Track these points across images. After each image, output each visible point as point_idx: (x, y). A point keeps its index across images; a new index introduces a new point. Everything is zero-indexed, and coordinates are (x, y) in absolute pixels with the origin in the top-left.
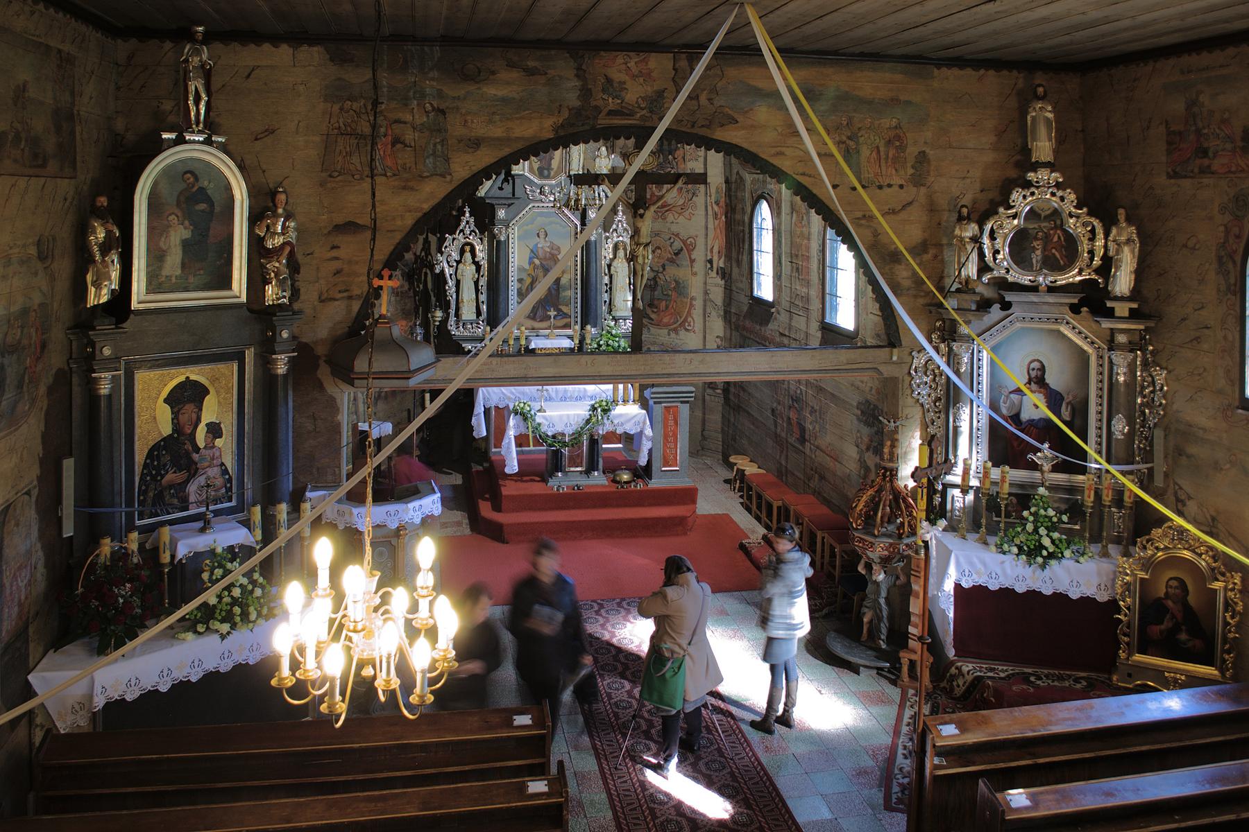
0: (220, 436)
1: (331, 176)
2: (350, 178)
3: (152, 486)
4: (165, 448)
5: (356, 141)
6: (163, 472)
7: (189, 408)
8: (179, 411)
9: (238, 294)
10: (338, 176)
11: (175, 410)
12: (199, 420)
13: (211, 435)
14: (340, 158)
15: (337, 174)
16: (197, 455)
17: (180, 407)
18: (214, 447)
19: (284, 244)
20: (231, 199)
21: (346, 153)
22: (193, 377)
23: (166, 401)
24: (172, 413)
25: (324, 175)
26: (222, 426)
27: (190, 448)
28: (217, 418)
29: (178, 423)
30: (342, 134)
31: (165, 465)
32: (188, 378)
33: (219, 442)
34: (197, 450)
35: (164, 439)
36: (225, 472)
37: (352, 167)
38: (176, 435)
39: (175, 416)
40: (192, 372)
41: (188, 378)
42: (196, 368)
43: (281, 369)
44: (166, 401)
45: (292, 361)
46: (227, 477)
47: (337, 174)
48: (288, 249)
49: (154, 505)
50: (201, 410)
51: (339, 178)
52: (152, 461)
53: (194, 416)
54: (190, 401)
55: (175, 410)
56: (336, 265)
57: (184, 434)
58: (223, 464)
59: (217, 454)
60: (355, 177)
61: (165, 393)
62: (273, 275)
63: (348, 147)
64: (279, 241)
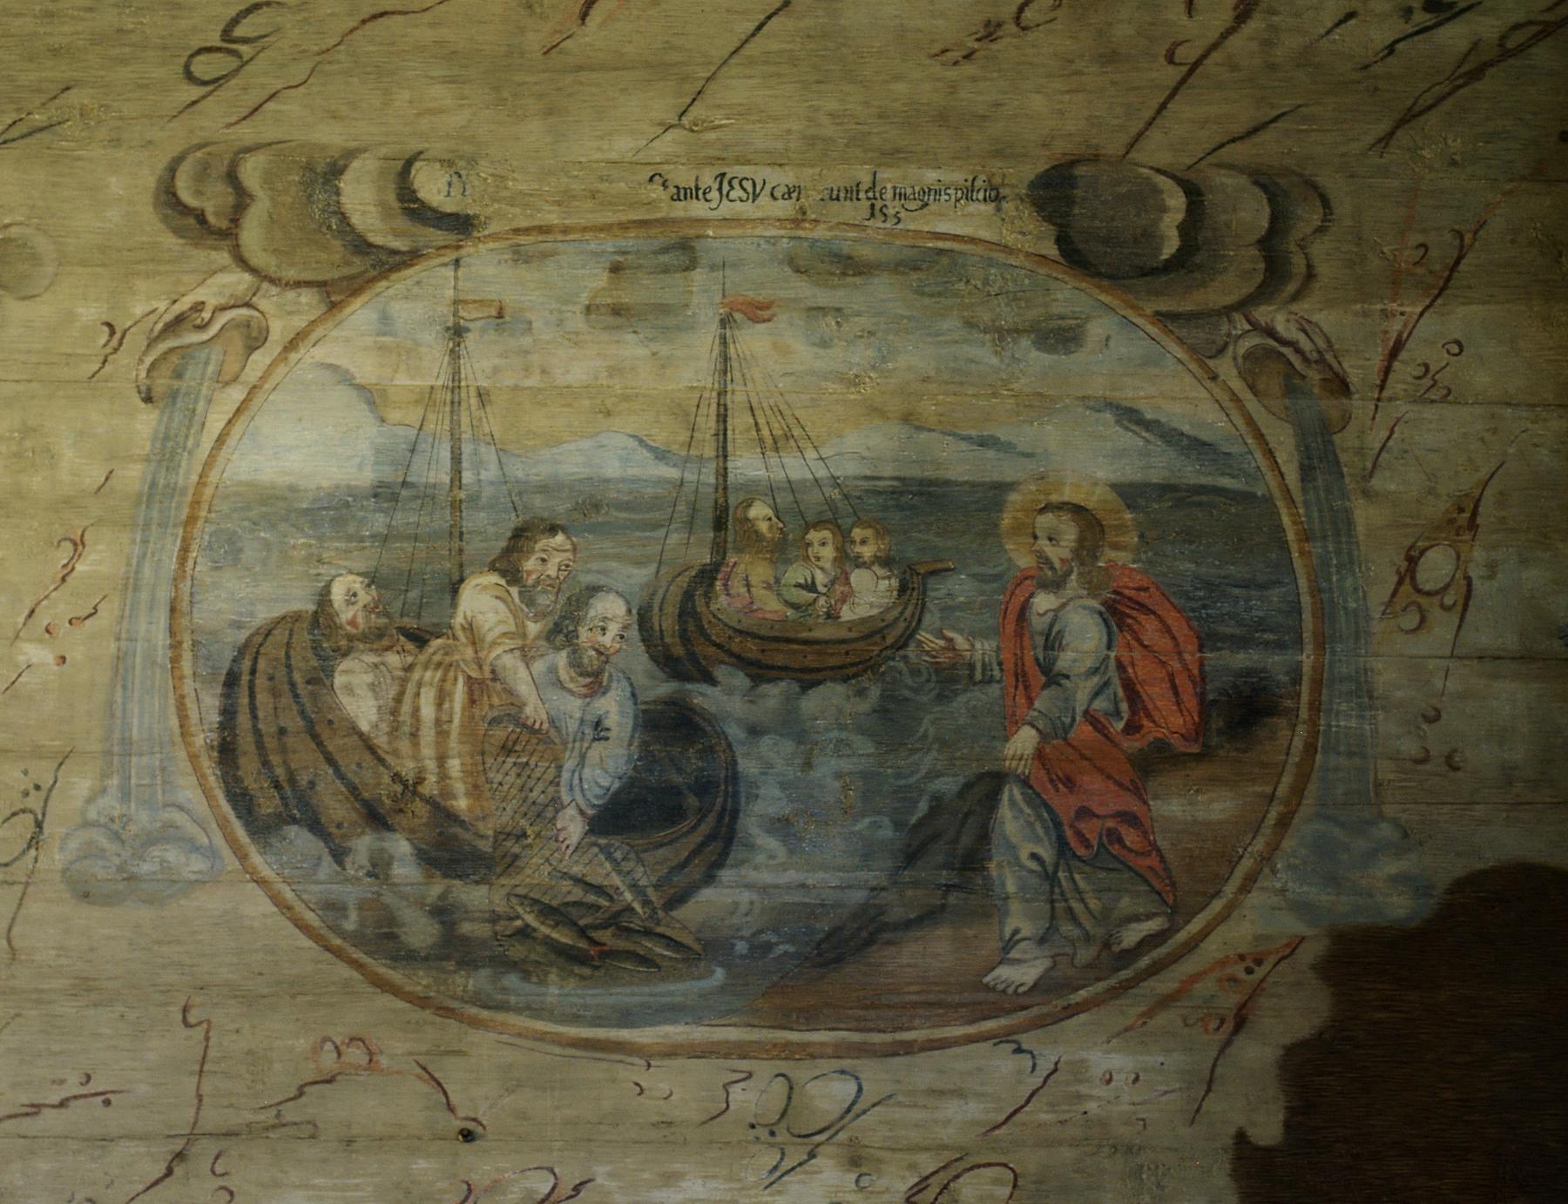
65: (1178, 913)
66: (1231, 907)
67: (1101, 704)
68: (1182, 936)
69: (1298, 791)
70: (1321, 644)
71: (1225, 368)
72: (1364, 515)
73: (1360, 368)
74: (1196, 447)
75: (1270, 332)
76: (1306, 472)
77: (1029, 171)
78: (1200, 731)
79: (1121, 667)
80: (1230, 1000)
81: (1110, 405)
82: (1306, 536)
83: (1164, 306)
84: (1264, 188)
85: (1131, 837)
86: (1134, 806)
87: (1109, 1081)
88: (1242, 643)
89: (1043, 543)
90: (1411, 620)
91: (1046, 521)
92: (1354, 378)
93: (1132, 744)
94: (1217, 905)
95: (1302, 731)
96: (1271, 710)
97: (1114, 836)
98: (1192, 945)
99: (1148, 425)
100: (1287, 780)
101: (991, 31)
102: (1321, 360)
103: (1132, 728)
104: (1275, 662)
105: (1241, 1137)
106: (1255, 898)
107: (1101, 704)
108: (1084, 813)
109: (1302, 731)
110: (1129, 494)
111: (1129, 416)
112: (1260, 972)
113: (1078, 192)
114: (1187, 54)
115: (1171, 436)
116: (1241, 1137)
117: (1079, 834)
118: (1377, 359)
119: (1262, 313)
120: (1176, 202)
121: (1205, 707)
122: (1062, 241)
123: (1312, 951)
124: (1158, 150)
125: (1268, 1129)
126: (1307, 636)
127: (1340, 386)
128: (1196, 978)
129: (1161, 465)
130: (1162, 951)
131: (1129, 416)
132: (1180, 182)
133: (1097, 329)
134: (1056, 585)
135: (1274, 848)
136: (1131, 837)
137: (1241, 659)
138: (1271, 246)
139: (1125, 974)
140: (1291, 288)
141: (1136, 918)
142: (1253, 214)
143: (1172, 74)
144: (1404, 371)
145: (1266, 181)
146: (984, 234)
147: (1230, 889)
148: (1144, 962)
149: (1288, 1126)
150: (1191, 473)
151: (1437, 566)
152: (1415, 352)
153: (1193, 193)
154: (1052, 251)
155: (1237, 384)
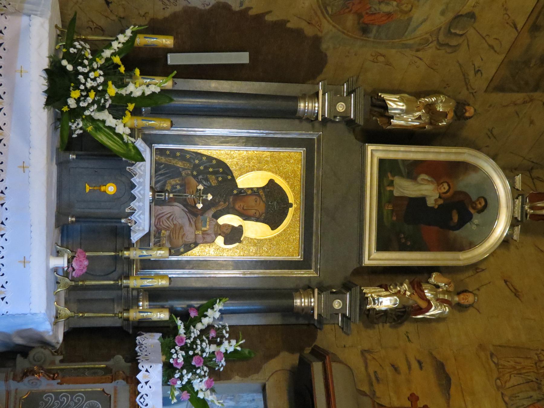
0: (226, 243)
1: (492, 355)
2: (495, 375)
3: (187, 165)
4: (225, 180)
5: (534, 380)
6: (200, 177)
7: (261, 208)
8: (259, 196)
9: (372, 257)
10: (494, 362)
11: (261, 192)
12: (246, 217)
13: (228, 232)
14: (512, 363)
15: (495, 360)
16: (211, 215)
17: (264, 199)
18: (217, 235)
19: (428, 301)
20: (461, 249)
21: (520, 369)
22: (291, 210)
23: (271, 182)
24: (258, 188)
25: (491, 348)
26: (237, 244)
27: (220, 208)
28: (245, 237)
29: (247, 195)
30: (536, 363)
31: (207, 180)
32: (291, 205)
33: (220, 240)
34: (216, 216)
35: (233, 180)
36: (188, 247)
37: (507, 376)
38: (235, 192)
39: (255, 192)
40: (296, 210)
41: (291, 205)
42: (300, 215)
43: (300, 302)
44: (271, 182)
45: (307, 313)
46: (182, 250)
47: (495, 360)
48: (423, 305)
49: (167, 166)
50: (257, 220)
51: (493, 365)
52: (212, 166)
53: (252, 212)
54: (267, 207)
55: (261, 192)
56: (403, 367)
57: (235, 201)
58: (196, 245)
59: (208, 238)
60: (498, 381)
61: (280, 181)
62: (394, 291)
63: (524, 371)
64: (428, 294)
65: (331, 16)
66: (330, 23)
67: (373, 9)
68: (327, 16)
69: (348, 35)
70: (373, 42)
71: (427, 36)
72: (393, 51)
73: (420, 54)
74: (415, 30)
75: (431, 43)
76: (405, 44)
77: (476, 11)
78: (364, 23)
79: (379, 13)
80: (314, 22)
81: (427, 19)
82: (393, 43)
83: (442, 29)
84: (458, 45)
85: (347, 10)
86: (352, 12)
87: (303, 3)
88: (377, 31)
89: (406, 5)
90: (374, 54)
91: (410, 6)
92: (418, 53)
93: (364, 13)
94: (331, 21)
95: (359, 37)
96: (363, 34)
97: (348, 8)
98: (325, 18)
99: (421, 23)
100: (350, 34)
101: (506, 9)
102: (423, 49)
103: (367, 13)
104: (372, 35)
105: (289, 21)
106: (331, 27)
107: (373, 9)
108: (353, 4)
109: (359, 37)
110: (410, 19)
111: (425, 20)
112: (317, 27)
113: (469, 19)
114: (487, 38)
115: (418, 26)
116: (289, 21)
117: (350, 3)
118: (419, 56)
119: (435, 43)
120: (461, 33)
121: (366, 24)
122: (461, 15)
123: (320, 34)
124: (471, 31)
125: (289, 25)
126: (375, 40)
127: (418, 50)
128: (319, 18)
129: (413, 24)
130: (325, 13)
131: (425, 20)
132: (464, 34)
133: (443, 19)
134: (397, 6)
135: (339, 30)
136: (347, 10)
137: (374, 31)
138: (447, 45)
139: (322, 7)
140: (438, 47)
141: (332, 9)
142: (454, 42)
143: (484, 35)
144: (417, 59)
145: (458, 45)
146: (468, 3)
147: (334, 23)
148: (324, 10)
149: (289, 28)
150: (410, 28)
151: (381, 59)
152: (419, 62)
153: (461, 35)
154: (460, 13)
155: (424, 37)
